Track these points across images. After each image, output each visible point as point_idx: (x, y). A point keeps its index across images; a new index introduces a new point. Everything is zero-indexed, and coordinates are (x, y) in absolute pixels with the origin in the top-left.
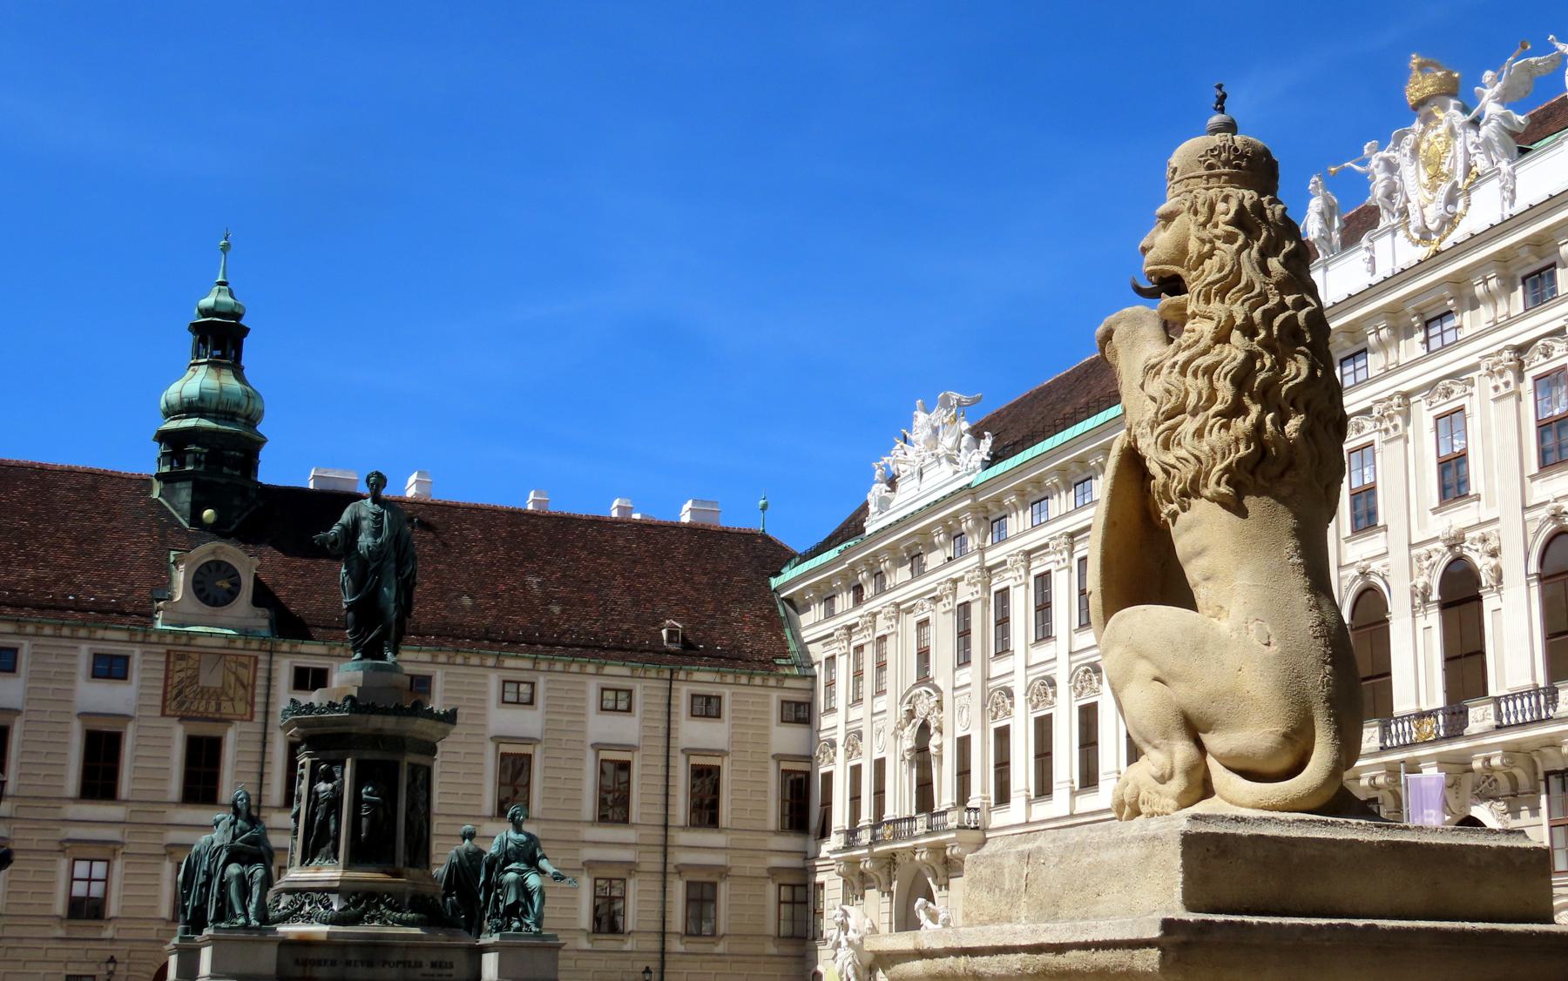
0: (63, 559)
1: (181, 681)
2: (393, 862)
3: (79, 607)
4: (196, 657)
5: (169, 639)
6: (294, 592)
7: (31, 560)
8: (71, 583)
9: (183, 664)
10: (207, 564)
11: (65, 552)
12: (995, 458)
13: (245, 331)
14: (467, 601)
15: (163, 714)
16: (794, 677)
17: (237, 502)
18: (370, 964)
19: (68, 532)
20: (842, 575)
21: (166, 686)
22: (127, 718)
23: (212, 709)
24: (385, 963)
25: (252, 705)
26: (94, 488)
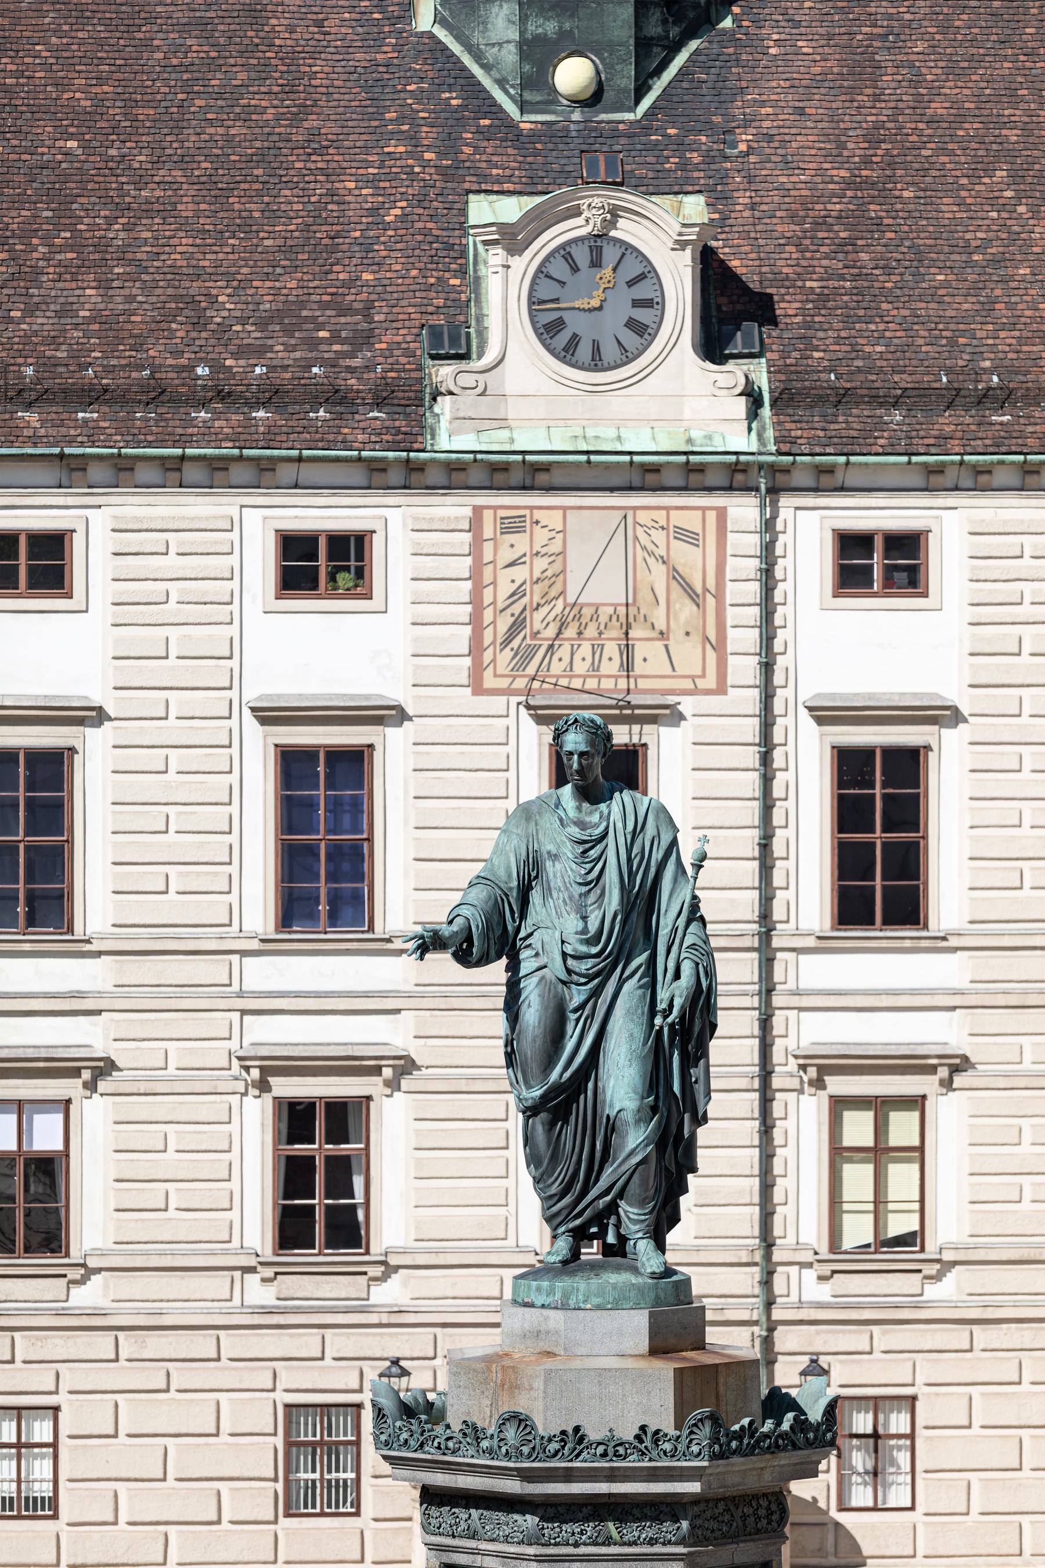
1: (516, 594)
3: (222, 395)
4: (554, 519)
5: (476, 476)
6: (822, 299)
7: (94, 259)
8: (199, 323)
9: (521, 543)
10: (564, 252)
11: (184, 226)
15: (478, 689)
21: (476, 600)
23: (611, 666)
25: (720, 647)
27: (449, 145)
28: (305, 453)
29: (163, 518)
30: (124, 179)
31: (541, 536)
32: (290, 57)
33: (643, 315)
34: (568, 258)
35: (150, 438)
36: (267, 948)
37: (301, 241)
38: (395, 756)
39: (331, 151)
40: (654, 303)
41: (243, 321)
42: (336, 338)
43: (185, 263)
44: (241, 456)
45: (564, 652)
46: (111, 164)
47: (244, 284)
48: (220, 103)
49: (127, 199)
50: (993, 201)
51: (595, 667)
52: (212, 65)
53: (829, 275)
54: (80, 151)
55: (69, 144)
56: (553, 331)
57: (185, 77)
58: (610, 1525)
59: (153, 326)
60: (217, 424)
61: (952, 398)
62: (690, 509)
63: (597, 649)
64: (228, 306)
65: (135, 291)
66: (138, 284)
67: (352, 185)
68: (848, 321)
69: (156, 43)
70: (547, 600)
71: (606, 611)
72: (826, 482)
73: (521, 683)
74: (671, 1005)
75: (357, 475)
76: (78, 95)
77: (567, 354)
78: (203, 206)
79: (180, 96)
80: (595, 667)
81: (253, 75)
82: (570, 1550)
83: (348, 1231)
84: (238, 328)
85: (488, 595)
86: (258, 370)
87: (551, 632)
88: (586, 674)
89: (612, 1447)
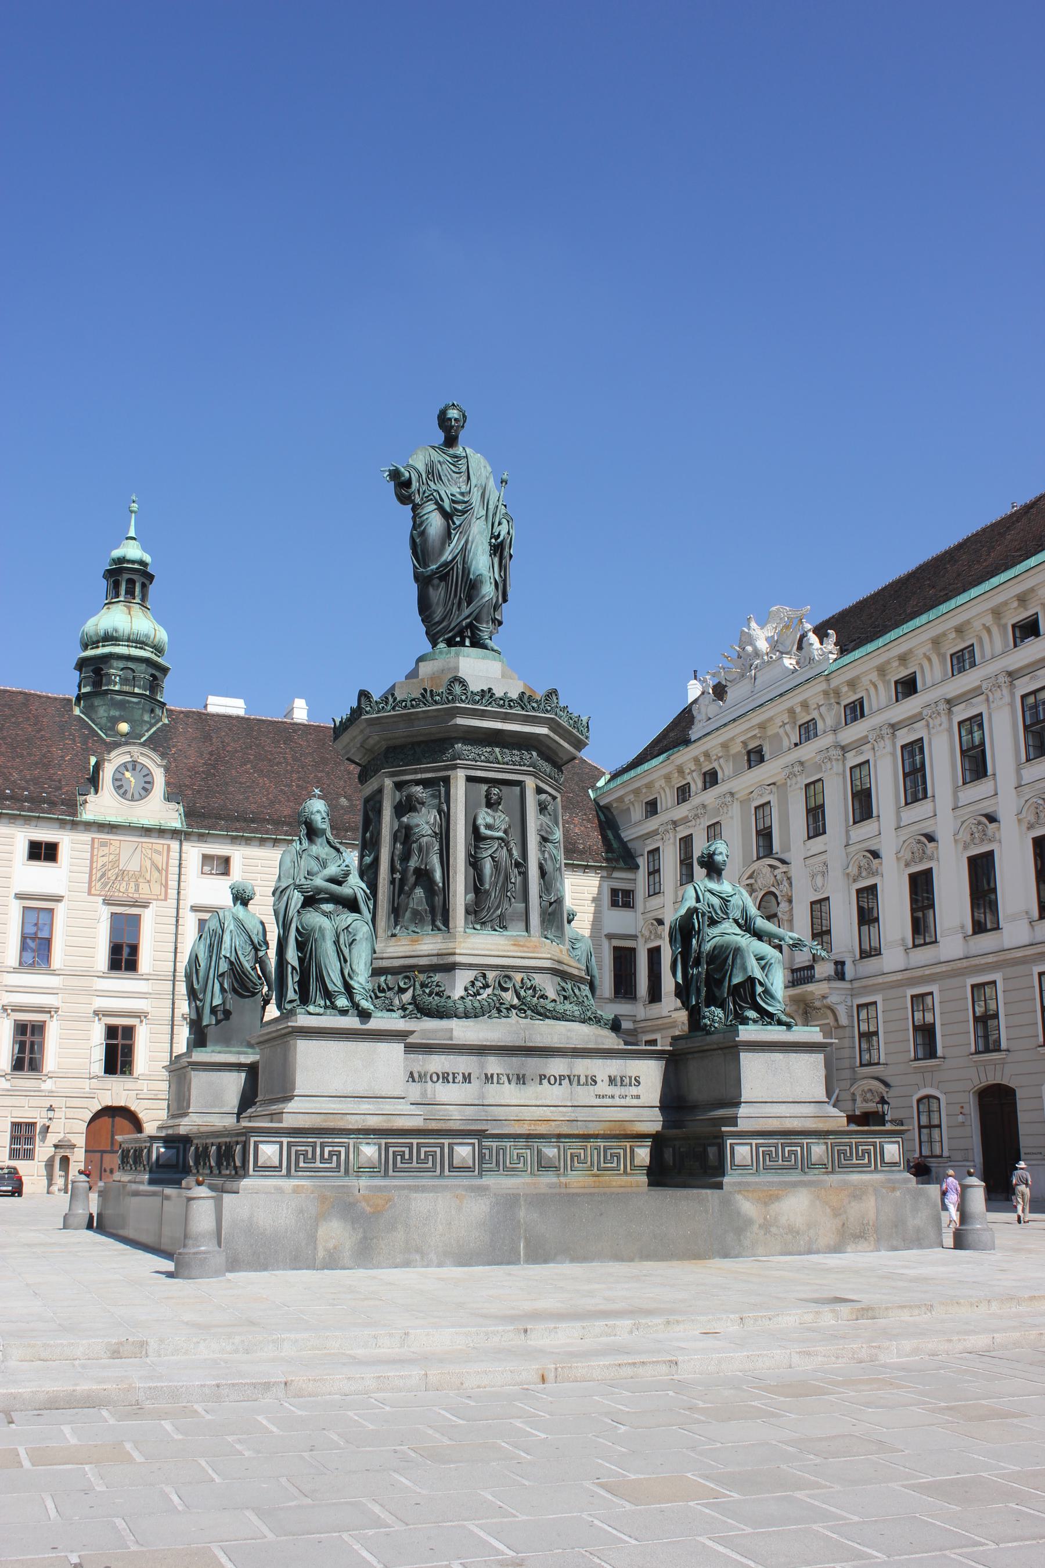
2: (527, 930)
6: (198, 792)
8: (7, 779)
9: (106, 850)
10: (125, 766)
12: (843, 651)
13: (150, 577)
14: (343, 801)
16: (621, 869)
17: (146, 718)
18: (521, 1079)
20: (668, 778)
22: (58, 899)
23: (132, 890)
24: (542, 1077)
25: (166, 886)
27: (85, 743)
31: (112, 848)
32: (36, 717)
33: (147, 786)
34: (126, 767)
36: (15, 971)
38: (61, 911)
40: (151, 783)
42: (50, 787)
45: (117, 884)
47: (21, 771)
50: (247, 773)
51: (127, 890)
53: (200, 786)
56: (119, 786)
58: (497, 750)
61: (237, 819)
62: (159, 843)
63: (128, 884)
68: (207, 797)
70: (113, 868)
71: (131, 873)
72: (202, 837)
73: (103, 893)
74: (499, 535)
75: (57, 825)
77: (124, 795)
80: (127, 890)
82: (473, 763)
83: (35, 1066)
85: (95, 865)
87: (113, 878)
88: (125, 890)
89: (506, 701)
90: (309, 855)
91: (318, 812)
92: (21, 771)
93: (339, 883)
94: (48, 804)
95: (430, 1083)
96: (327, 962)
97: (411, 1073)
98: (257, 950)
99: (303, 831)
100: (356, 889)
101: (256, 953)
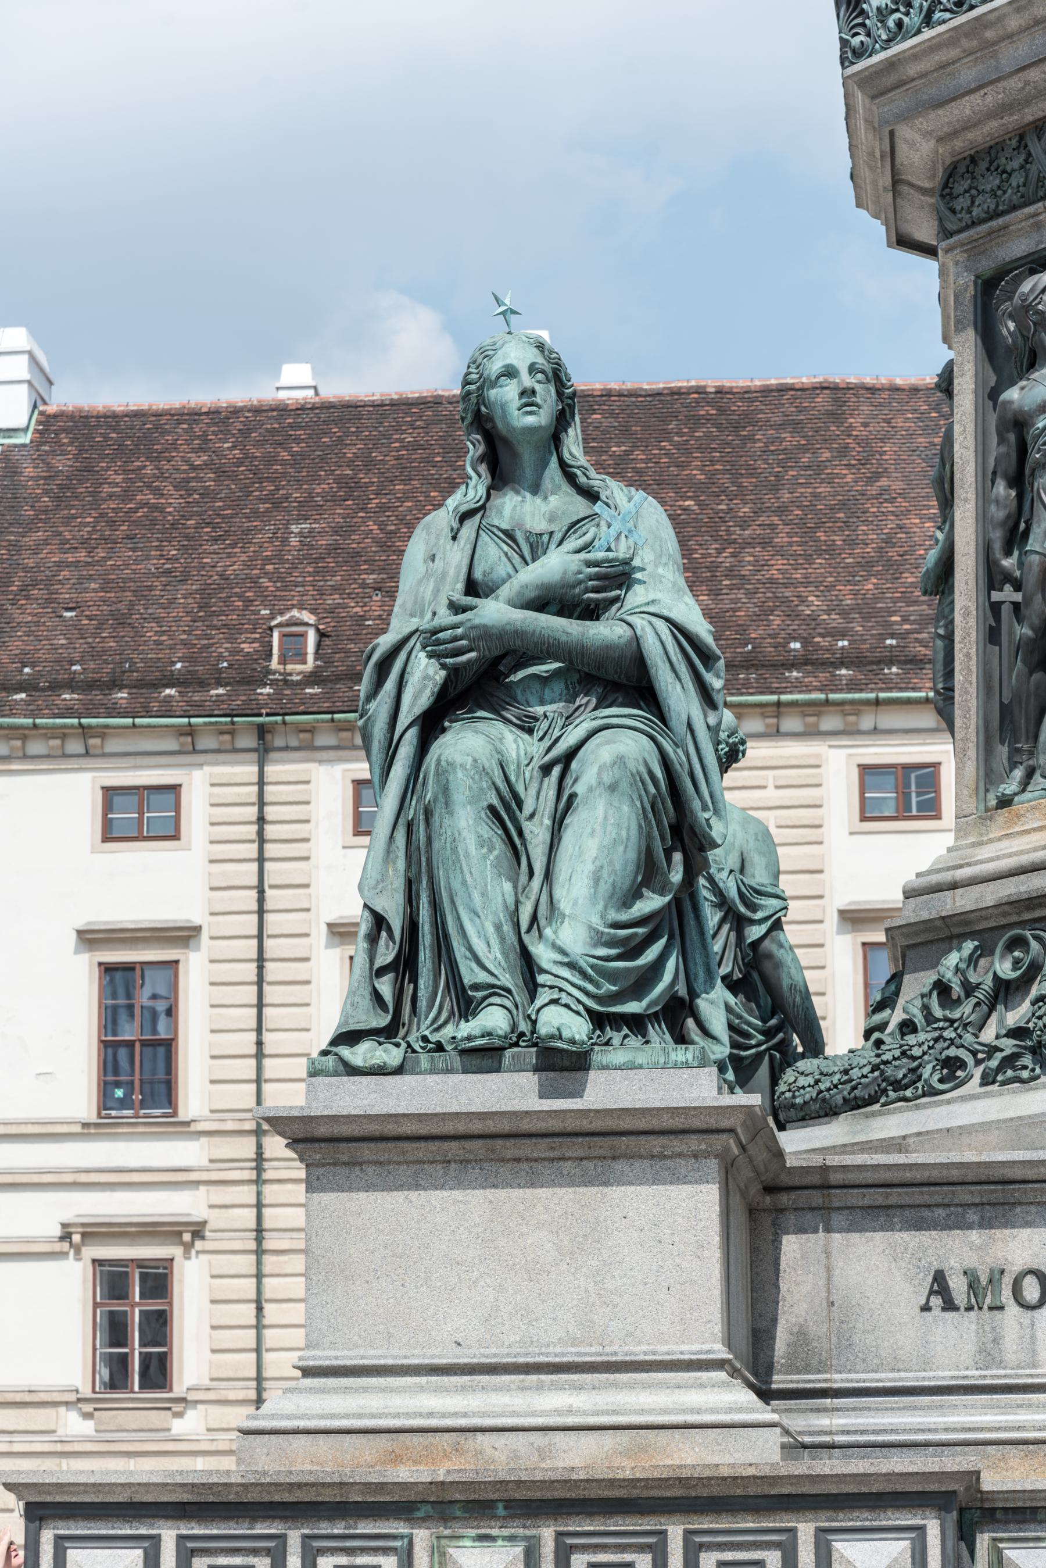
0: (777, 567)
8: (793, 614)
11: (780, 551)
19: (782, 510)
26: (836, 416)
28: (882, 695)
29: (764, 758)
30: (731, 524)
32: (864, 443)
35: (751, 691)
37: (876, 559)
39: (899, 500)
41: (828, 612)
42: (905, 620)
43: (781, 576)
44: (827, 700)
46: (721, 515)
48: (809, 472)
49: (734, 537)
52: (804, 449)
54: (696, 507)
55: (687, 503)
57: (781, 457)
59: (754, 618)
60: (806, 680)
64: (816, 603)
65: (739, 596)
66: (742, 591)
67: (917, 521)
69: (757, 437)
76: (694, 472)
78: (795, 539)
79: (776, 470)
81: (835, 454)
84: (825, 617)
86: (840, 644)
90: (491, 529)
91: (510, 372)
92: (830, 588)
93: (592, 612)
94: (900, 663)
95: (1013, 1309)
96: (456, 885)
97: (939, 1277)
98: (739, 923)
99: (475, 447)
100: (638, 621)
101: (740, 938)
